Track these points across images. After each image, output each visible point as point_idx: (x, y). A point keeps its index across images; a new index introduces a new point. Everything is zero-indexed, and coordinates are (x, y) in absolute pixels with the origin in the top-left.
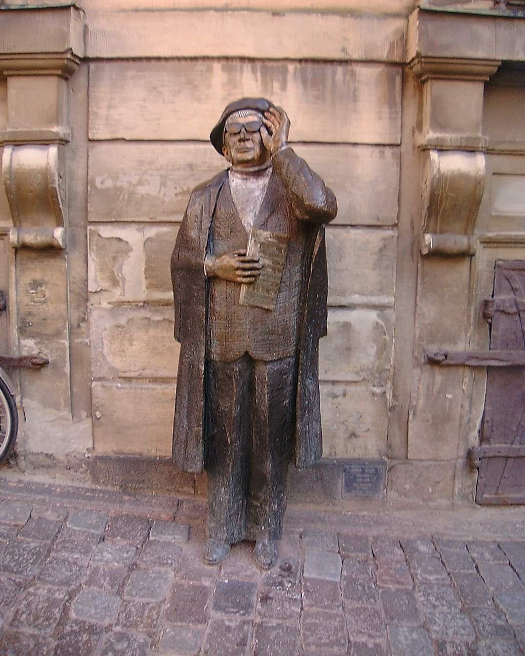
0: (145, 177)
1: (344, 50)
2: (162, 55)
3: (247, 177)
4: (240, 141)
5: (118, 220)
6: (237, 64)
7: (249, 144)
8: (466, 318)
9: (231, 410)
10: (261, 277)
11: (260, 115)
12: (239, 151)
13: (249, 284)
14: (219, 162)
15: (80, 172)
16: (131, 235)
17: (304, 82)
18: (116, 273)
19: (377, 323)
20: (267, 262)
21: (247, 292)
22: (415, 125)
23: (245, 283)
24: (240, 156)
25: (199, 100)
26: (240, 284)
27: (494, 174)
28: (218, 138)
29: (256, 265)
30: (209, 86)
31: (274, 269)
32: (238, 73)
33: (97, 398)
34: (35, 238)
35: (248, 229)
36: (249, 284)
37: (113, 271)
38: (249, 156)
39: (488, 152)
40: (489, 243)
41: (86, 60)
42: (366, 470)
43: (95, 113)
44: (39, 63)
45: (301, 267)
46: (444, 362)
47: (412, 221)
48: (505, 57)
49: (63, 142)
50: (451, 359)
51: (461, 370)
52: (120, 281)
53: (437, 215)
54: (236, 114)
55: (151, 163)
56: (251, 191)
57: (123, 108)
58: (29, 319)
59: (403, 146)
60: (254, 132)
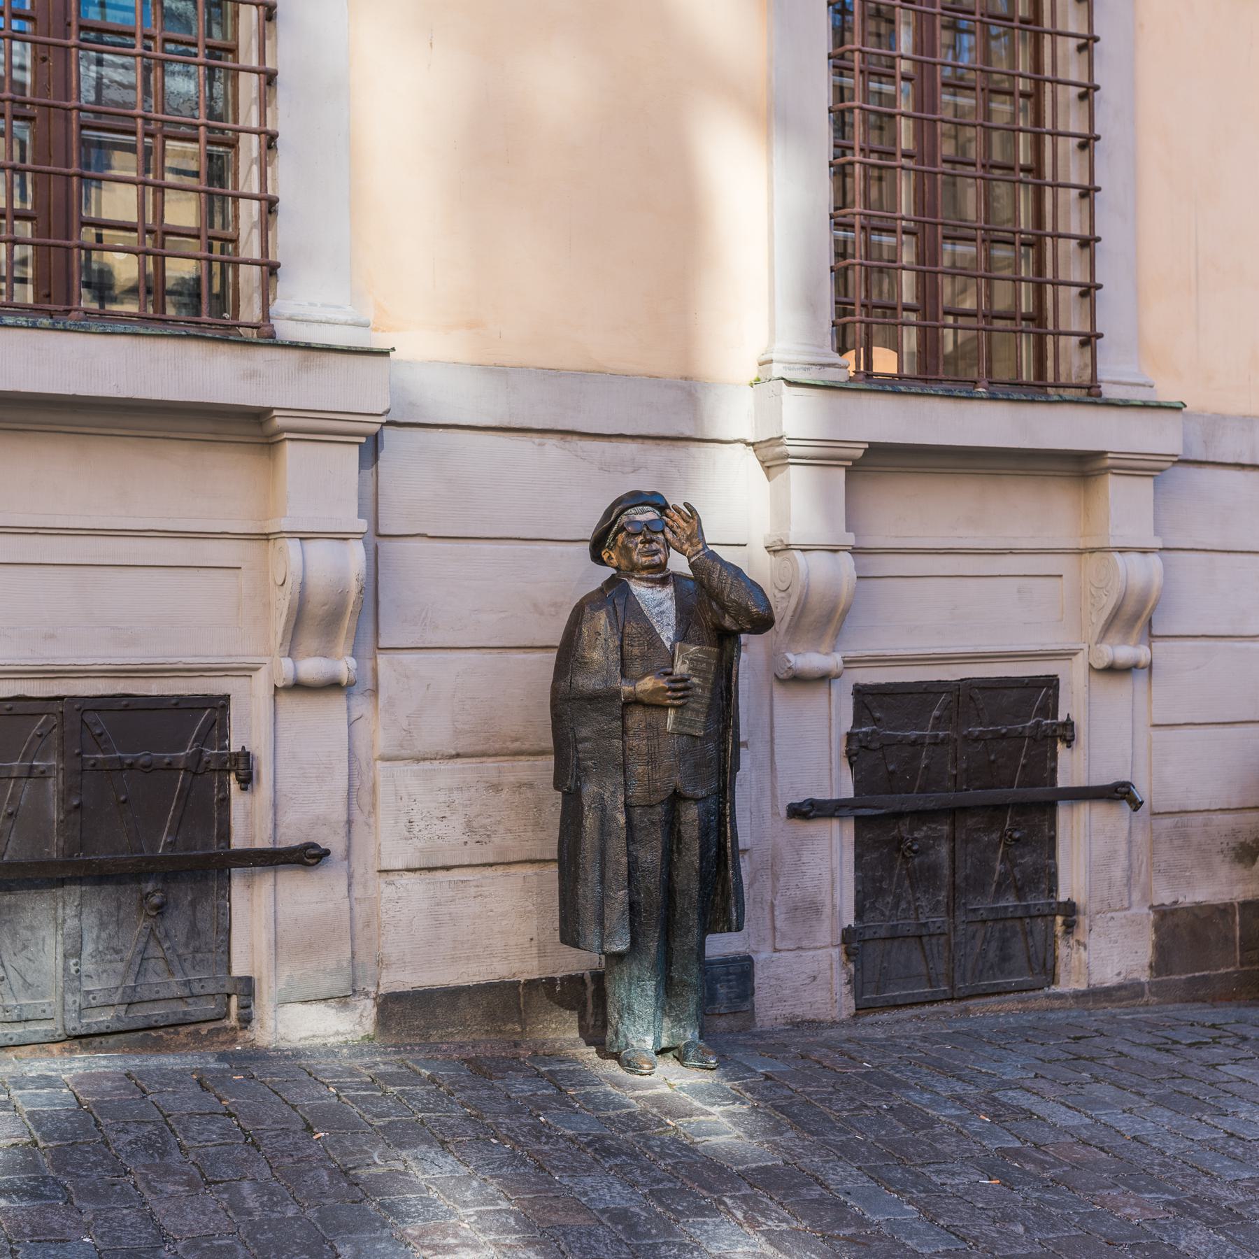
7: (654, 546)
21: (676, 718)
23: (673, 706)
31: (703, 688)
36: (676, 707)
54: (632, 511)
60: (657, 532)
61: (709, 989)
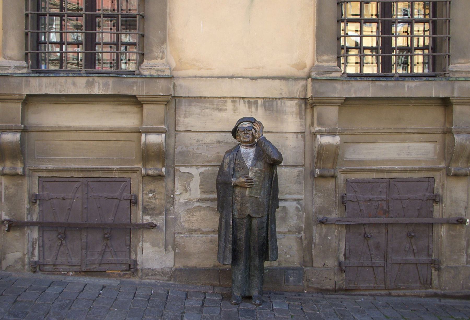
1: (281, 94)
4: (244, 134)
7: (248, 135)
12: (244, 138)
14: (236, 142)
15: (172, 144)
16: (194, 171)
17: (265, 107)
20: (257, 179)
21: (249, 191)
24: (245, 140)
25: (222, 115)
26: (246, 188)
28: (235, 133)
31: (259, 182)
32: (238, 104)
34: (154, 172)
35: (249, 167)
38: (248, 140)
39: (341, 134)
40: (343, 171)
41: (175, 97)
42: (295, 272)
43: (178, 120)
44: (158, 99)
51: (334, 226)
54: (242, 124)
55: (202, 141)
56: (249, 153)
58: (148, 207)
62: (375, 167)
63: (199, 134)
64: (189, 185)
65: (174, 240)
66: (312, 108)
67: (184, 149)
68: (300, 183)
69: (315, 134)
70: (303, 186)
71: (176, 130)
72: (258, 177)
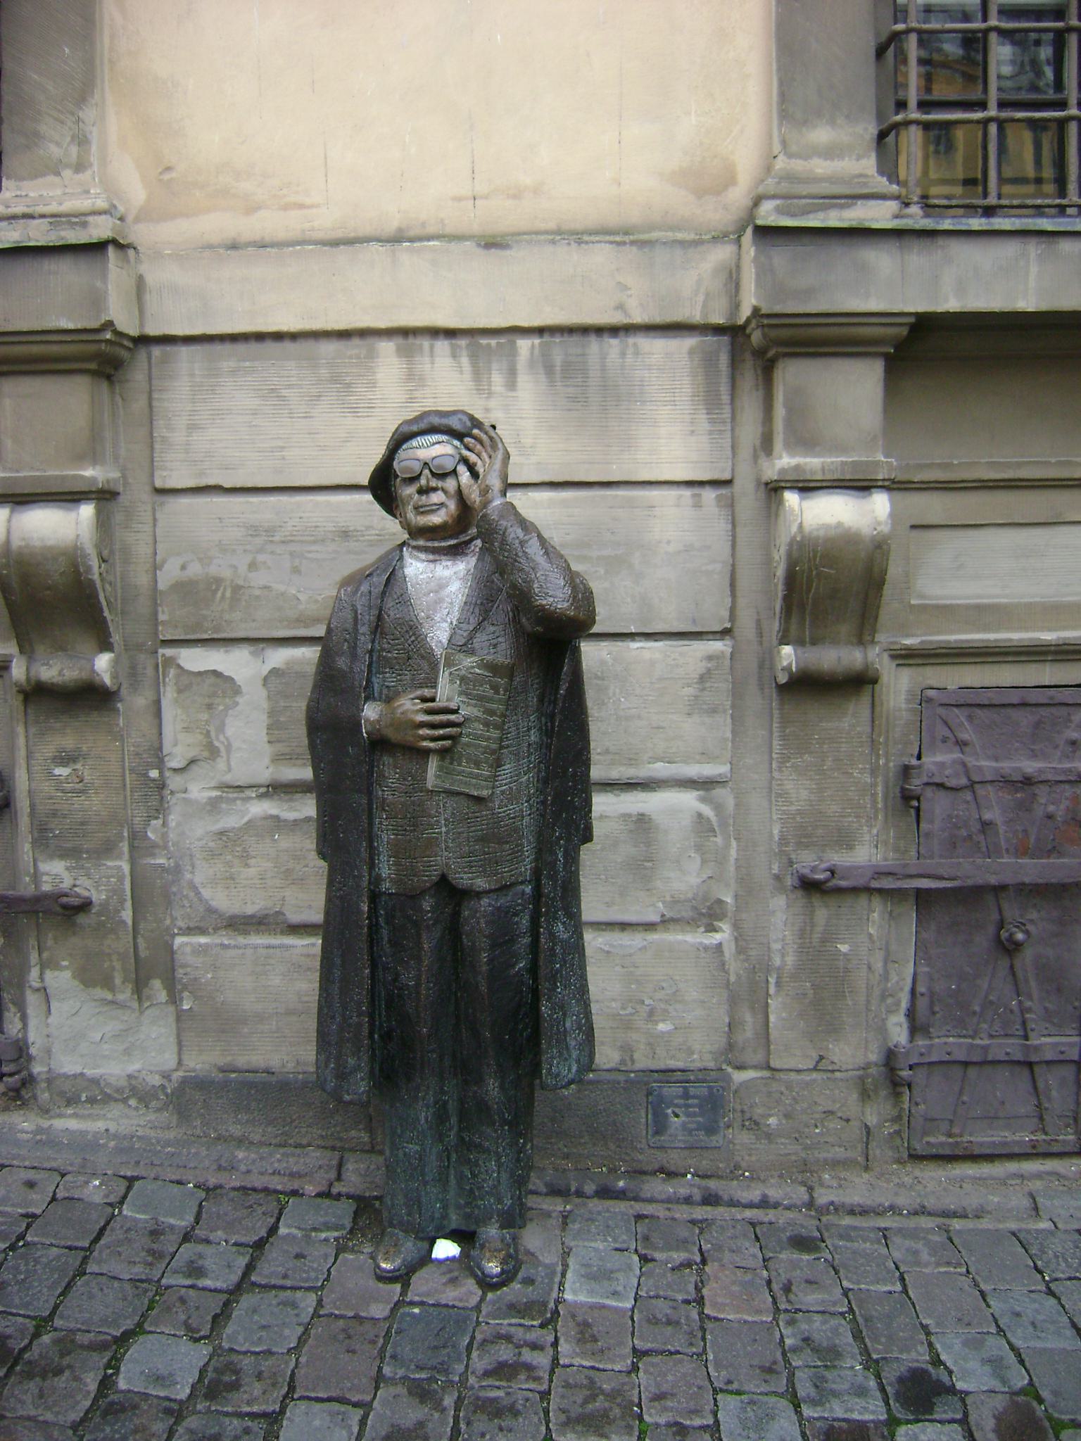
0: (261, 558)
1: (620, 307)
2: (284, 328)
3: (437, 557)
4: (422, 491)
5: (215, 636)
6: (426, 343)
7: (436, 498)
8: (868, 799)
9: (418, 985)
10: (465, 740)
11: (456, 443)
13: (443, 752)
15: (142, 549)
16: (237, 664)
17: (549, 370)
18: (213, 734)
19: (700, 815)
21: (440, 768)
22: (758, 443)
24: (423, 520)
25: (354, 411)
26: (427, 752)
27: (913, 527)
29: (452, 717)
30: (373, 385)
31: (487, 724)
32: (427, 359)
33: (184, 966)
34: (61, 673)
35: (438, 651)
37: (208, 732)
38: (437, 519)
39: (893, 486)
40: (906, 657)
41: (144, 341)
42: (692, 1091)
43: (164, 440)
45: (539, 719)
46: (830, 884)
47: (758, 622)
48: (921, 308)
49: (104, 496)
50: (842, 878)
51: (863, 900)
52: (222, 749)
53: (802, 606)
54: (414, 443)
55: (270, 531)
56: (442, 586)
57: (217, 426)
59: (738, 483)
61: (654, 1114)
62: (1048, 636)
63: (255, 499)
64: (221, 728)
65: (173, 960)
66: (767, 370)
67: (195, 570)
68: (713, 711)
69: (774, 490)
70: (724, 726)
71: (158, 484)
72: (481, 698)
